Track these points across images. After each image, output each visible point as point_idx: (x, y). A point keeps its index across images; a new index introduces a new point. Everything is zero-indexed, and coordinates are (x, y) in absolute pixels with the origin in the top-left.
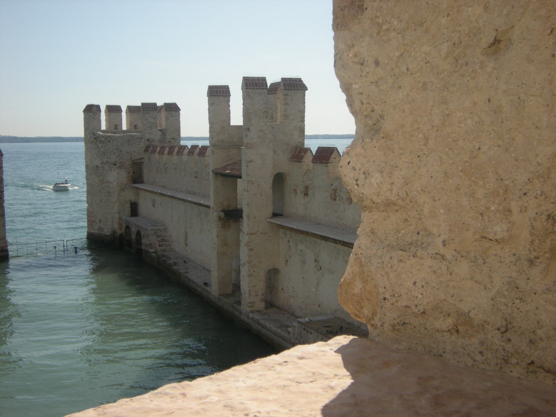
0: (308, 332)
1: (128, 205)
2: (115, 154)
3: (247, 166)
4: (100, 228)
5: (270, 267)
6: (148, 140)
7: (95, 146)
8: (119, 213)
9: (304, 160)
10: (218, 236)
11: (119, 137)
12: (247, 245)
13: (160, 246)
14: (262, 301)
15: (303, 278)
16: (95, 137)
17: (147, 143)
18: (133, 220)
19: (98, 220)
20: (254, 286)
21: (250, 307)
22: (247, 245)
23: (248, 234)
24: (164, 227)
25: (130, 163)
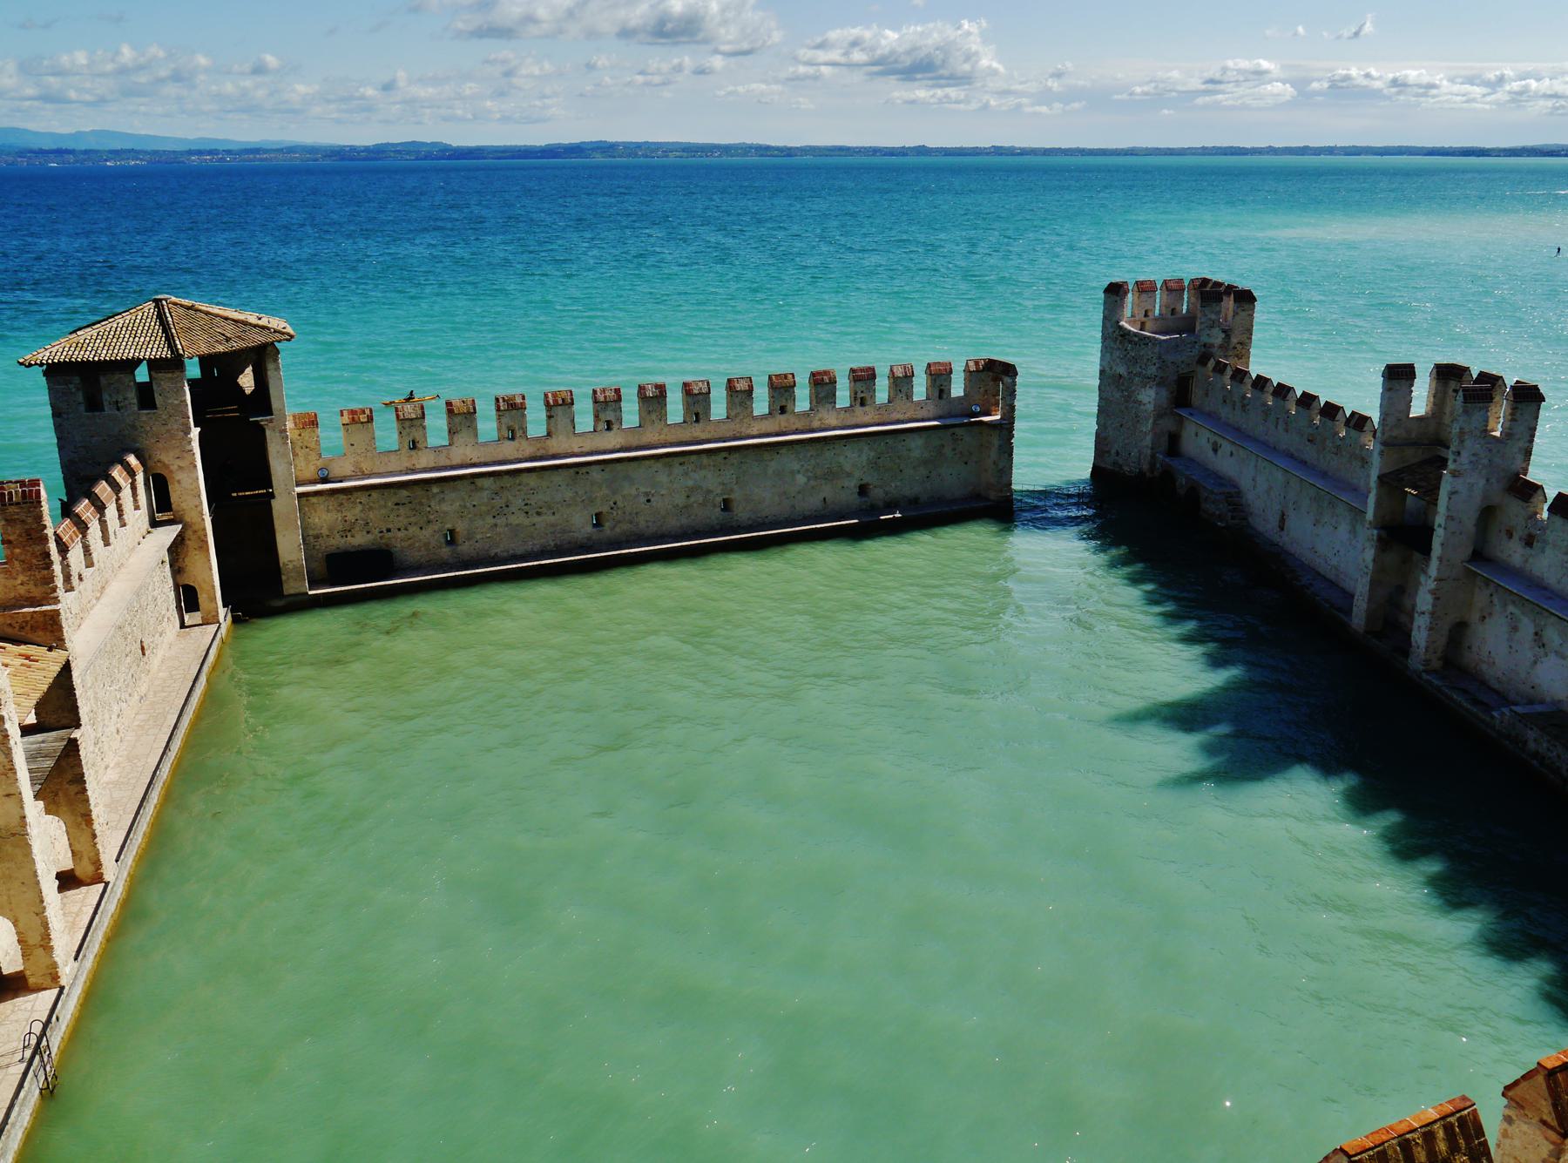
0: (1526, 725)
1: (1166, 438)
2: (1155, 364)
3: (1450, 498)
4: (1115, 463)
5: (1458, 620)
6: (1205, 345)
7: (1120, 347)
8: (1152, 449)
9: (1532, 500)
10: (1374, 560)
11: (1164, 340)
12: (1432, 592)
13: (1233, 518)
14: (1439, 659)
15: (1511, 647)
16: (1121, 333)
17: (1203, 349)
18: (1175, 463)
19: (1113, 451)
20: (1434, 642)
21: (1424, 665)
22: (1432, 592)
23: (1435, 580)
24: (1237, 490)
25: (1175, 378)
